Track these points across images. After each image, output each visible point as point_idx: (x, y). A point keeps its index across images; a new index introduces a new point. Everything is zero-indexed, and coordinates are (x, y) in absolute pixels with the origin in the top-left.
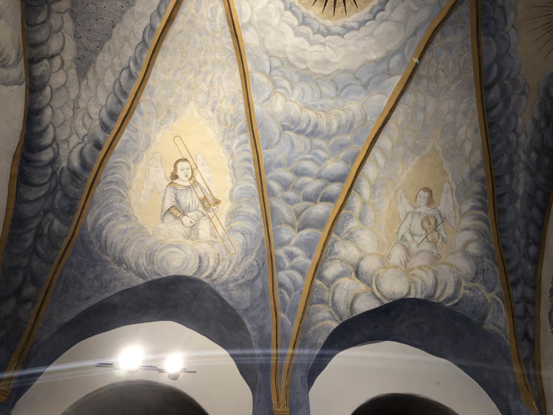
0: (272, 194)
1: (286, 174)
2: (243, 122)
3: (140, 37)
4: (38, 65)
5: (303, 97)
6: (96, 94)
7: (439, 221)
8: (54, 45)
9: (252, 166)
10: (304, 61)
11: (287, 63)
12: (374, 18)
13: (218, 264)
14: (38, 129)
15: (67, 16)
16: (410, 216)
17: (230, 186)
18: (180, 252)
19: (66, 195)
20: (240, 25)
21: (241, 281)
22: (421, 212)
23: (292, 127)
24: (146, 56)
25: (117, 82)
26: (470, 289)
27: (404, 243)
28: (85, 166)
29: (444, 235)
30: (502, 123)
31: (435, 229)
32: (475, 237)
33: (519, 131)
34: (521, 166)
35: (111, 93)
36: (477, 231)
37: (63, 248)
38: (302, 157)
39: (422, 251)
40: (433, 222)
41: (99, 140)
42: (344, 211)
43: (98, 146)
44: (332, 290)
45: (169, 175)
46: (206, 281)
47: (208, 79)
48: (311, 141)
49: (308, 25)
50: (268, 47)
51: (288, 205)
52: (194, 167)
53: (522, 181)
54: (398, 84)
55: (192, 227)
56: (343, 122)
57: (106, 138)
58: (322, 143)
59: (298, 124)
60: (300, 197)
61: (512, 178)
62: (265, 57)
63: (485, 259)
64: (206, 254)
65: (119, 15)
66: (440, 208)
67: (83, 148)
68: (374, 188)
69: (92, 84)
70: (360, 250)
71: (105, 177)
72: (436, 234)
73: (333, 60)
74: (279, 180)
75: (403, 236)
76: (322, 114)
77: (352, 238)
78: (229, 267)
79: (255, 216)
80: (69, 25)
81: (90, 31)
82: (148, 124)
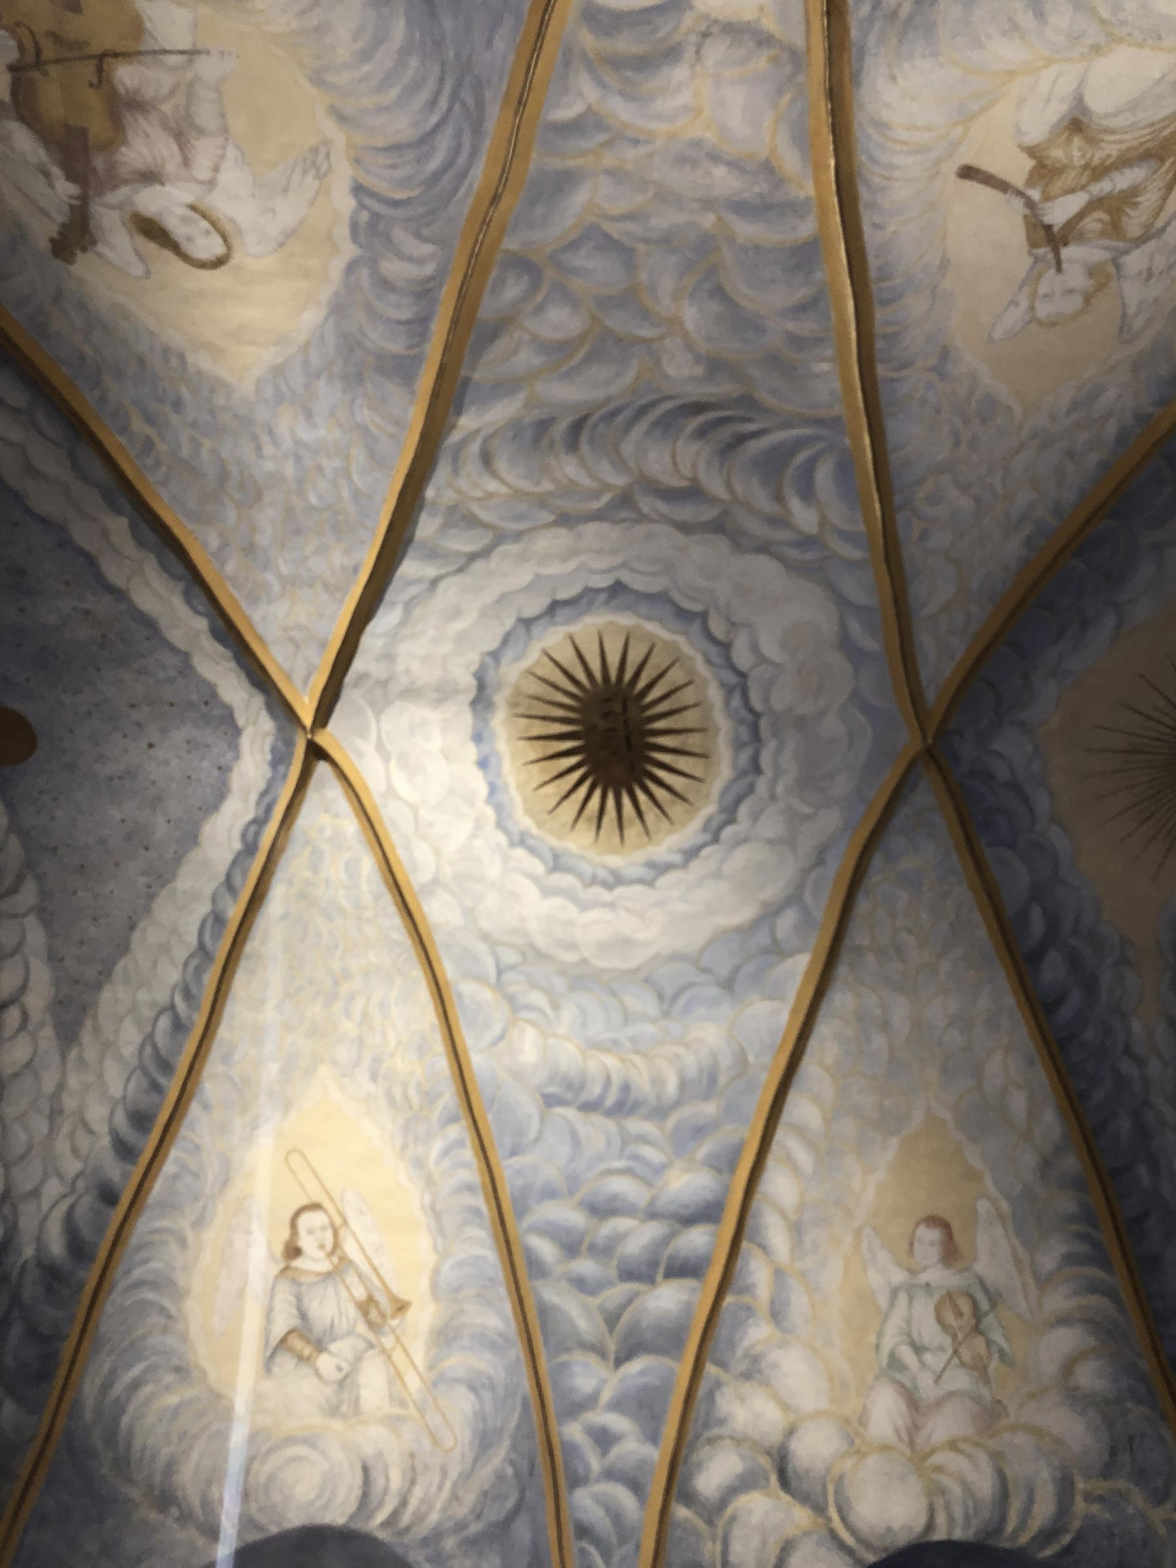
0: (538, 1268)
1: (571, 1216)
2: (449, 1096)
3: (193, 940)
5: (584, 1025)
6: (101, 1076)
7: (984, 1305)
9: (480, 1202)
10: (573, 946)
11: (533, 954)
12: (716, 839)
13: (413, 1482)
15: (31, 922)
16: (903, 1298)
17: (430, 1259)
18: (314, 1455)
19: (32, 1332)
20: (416, 888)
21: (475, 1528)
23: (569, 1096)
24: (210, 978)
26: (1101, 1499)
27: (898, 1376)
28: (79, 1249)
30: (1089, 1035)
31: (977, 1329)
32: (1091, 1342)
35: (135, 1070)
36: (1091, 1323)
37: (24, 1474)
38: (603, 1167)
39: (951, 1394)
40: (965, 1306)
42: (729, 1300)
43: (109, 1196)
44: (720, 1531)
45: (279, 1249)
46: (382, 1535)
47: (357, 1008)
48: (622, 1131)
49: (569, 870)
50: (485, 925)
51: (582, 1296)
52: (338, 1221)
54: (808, 972)
55: (341, 1384)
56: (692, 1073)
57: (126, 1176)
58: (648, 1128)
59: (582, 1086)
60: (613, 1273)
62: (482, 948)
63: (1129, 1405)
64: (380, 1454)
66: (980, 1267)
67: (72, 1207)
68: (799, 1232)
69: (91, 1054)
70: (785, 1407)
71: (128, 1271)
72: (979, 1343)
73: (641, 936)
74: (554, 1233)
75: (892, 1355)
76: (637, 1059)
77: (759, 1371)
78: (440, 1487)
79: (501, 1335)
80: (36, 936)
82: (223, 1129)
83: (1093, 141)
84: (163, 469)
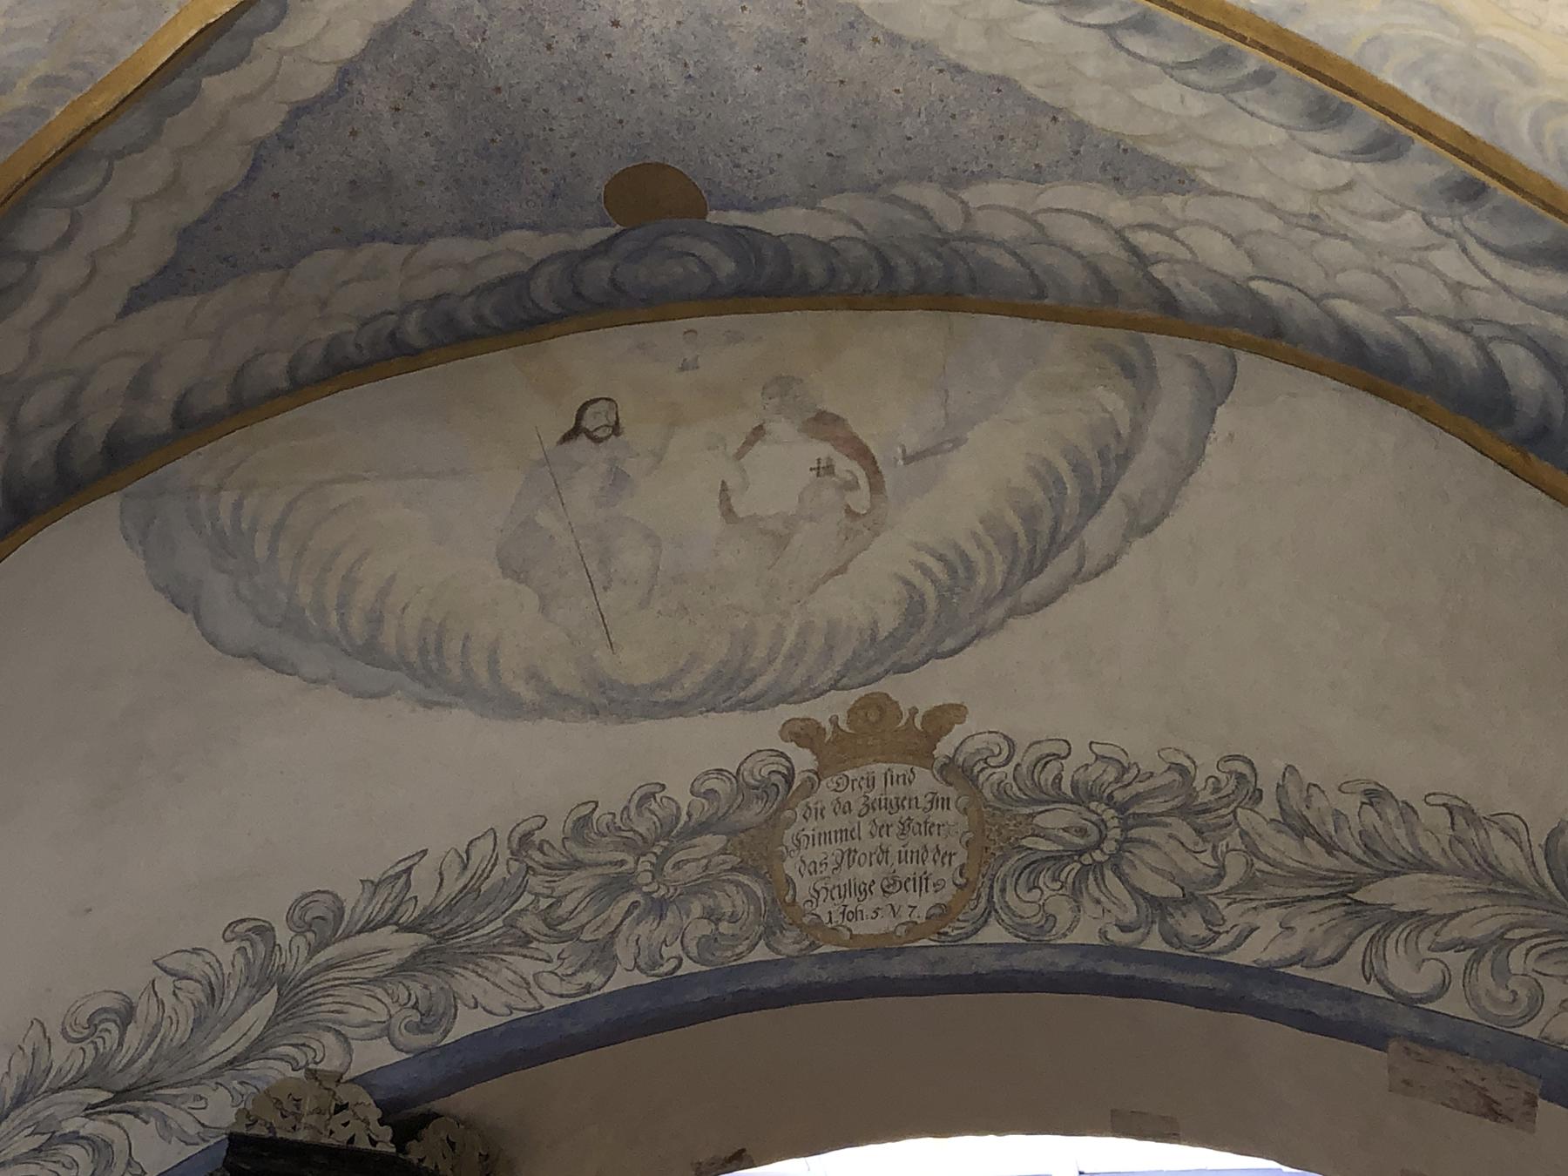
4: (1175, 291)
8: (1089, 239)
14: (1419, 363)
25: (1176, 73)
41: (1441, 180)
65: (908, 52)
67: (1485, 244)
80: (1000, 193)
81: (1002, 138)
84: (88, 59)
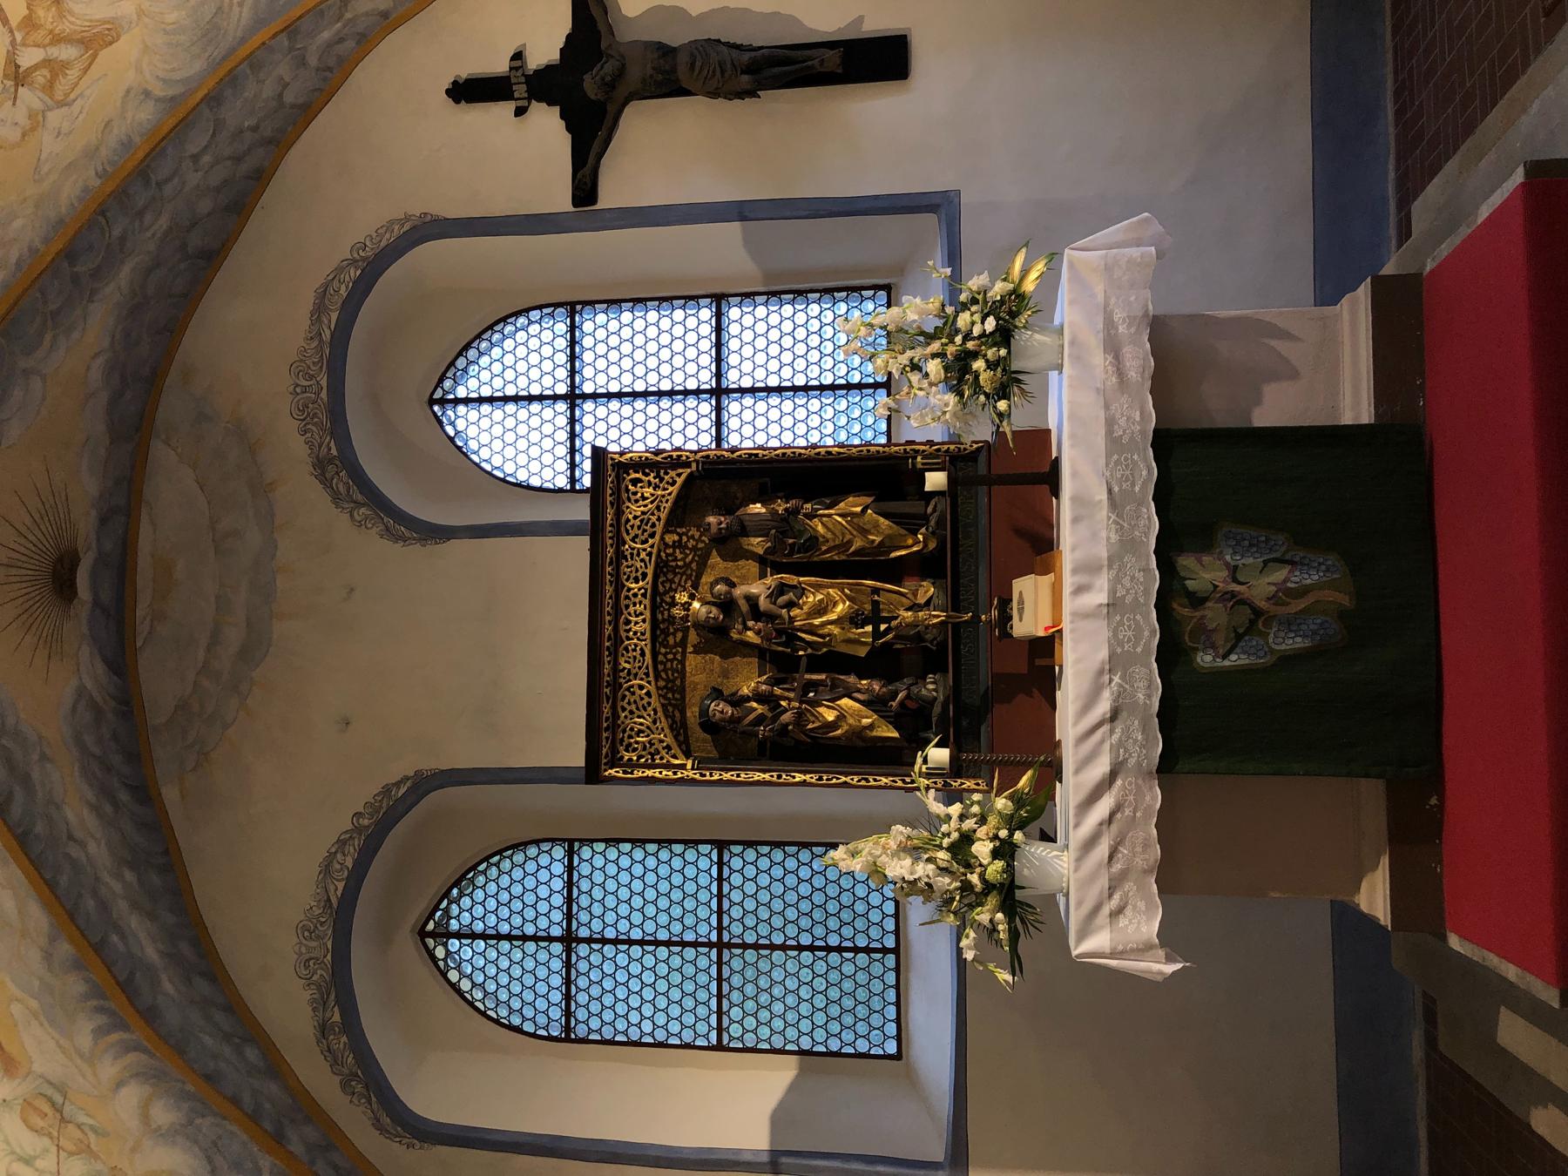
7: (58, 1099)
22: (8, 1099)
29: (91, 1122)
30: (39, 828)
31: (63, 1119)
32: (146, 1090)
33: (78, 834)
34: (123, 905)
36: (139, 1075)
40: (46, 1108)
53: (142, 936)
61: (123, 936)
63: (198, 1121)
83: (61, 16)
